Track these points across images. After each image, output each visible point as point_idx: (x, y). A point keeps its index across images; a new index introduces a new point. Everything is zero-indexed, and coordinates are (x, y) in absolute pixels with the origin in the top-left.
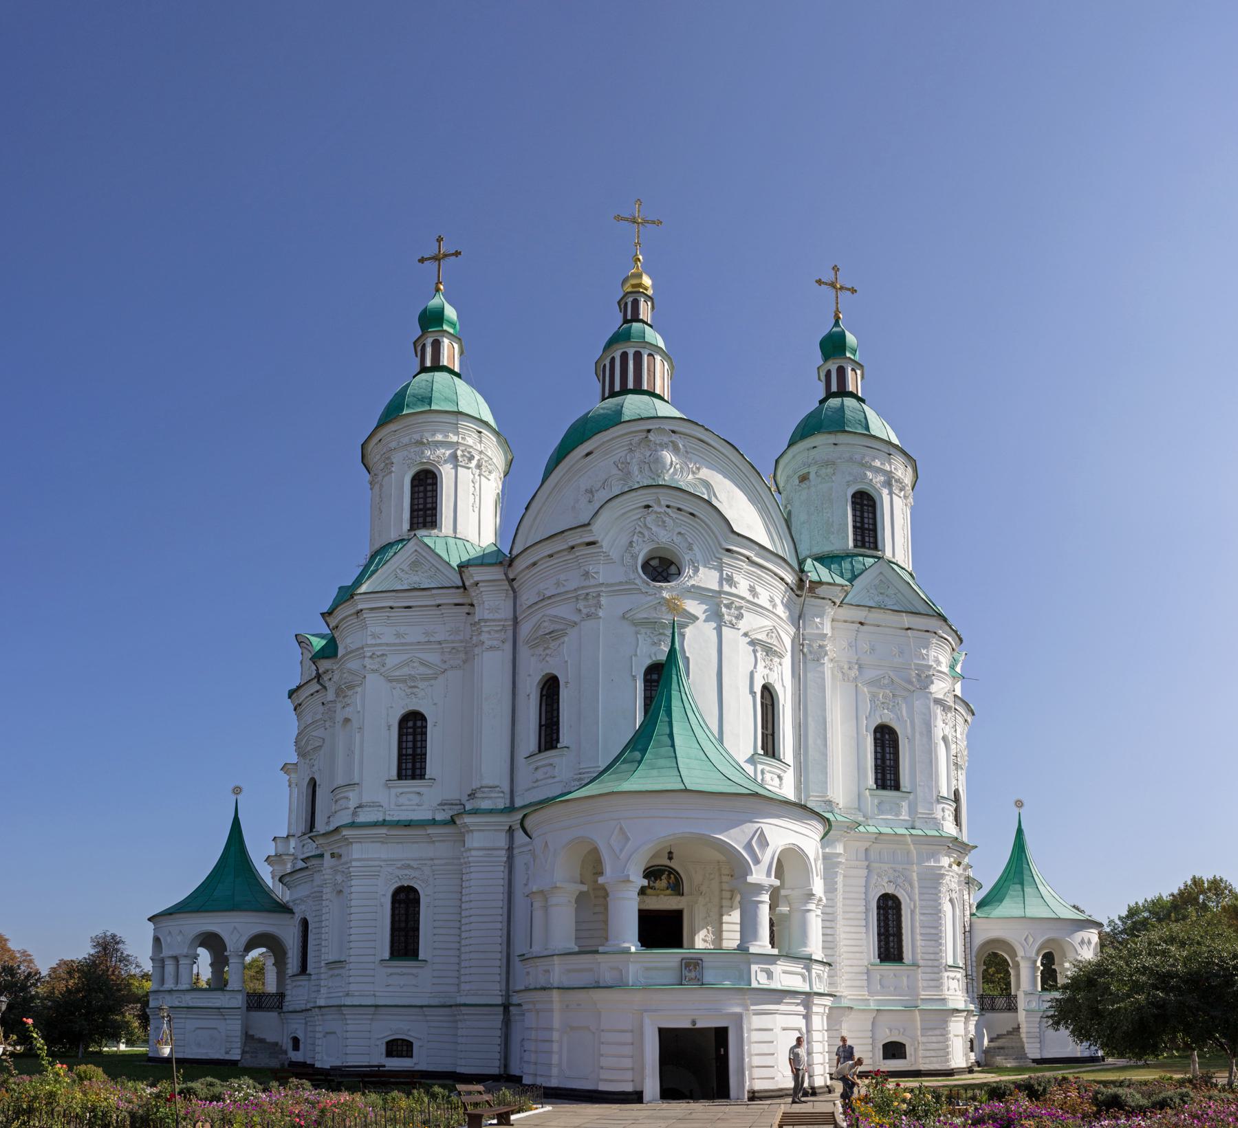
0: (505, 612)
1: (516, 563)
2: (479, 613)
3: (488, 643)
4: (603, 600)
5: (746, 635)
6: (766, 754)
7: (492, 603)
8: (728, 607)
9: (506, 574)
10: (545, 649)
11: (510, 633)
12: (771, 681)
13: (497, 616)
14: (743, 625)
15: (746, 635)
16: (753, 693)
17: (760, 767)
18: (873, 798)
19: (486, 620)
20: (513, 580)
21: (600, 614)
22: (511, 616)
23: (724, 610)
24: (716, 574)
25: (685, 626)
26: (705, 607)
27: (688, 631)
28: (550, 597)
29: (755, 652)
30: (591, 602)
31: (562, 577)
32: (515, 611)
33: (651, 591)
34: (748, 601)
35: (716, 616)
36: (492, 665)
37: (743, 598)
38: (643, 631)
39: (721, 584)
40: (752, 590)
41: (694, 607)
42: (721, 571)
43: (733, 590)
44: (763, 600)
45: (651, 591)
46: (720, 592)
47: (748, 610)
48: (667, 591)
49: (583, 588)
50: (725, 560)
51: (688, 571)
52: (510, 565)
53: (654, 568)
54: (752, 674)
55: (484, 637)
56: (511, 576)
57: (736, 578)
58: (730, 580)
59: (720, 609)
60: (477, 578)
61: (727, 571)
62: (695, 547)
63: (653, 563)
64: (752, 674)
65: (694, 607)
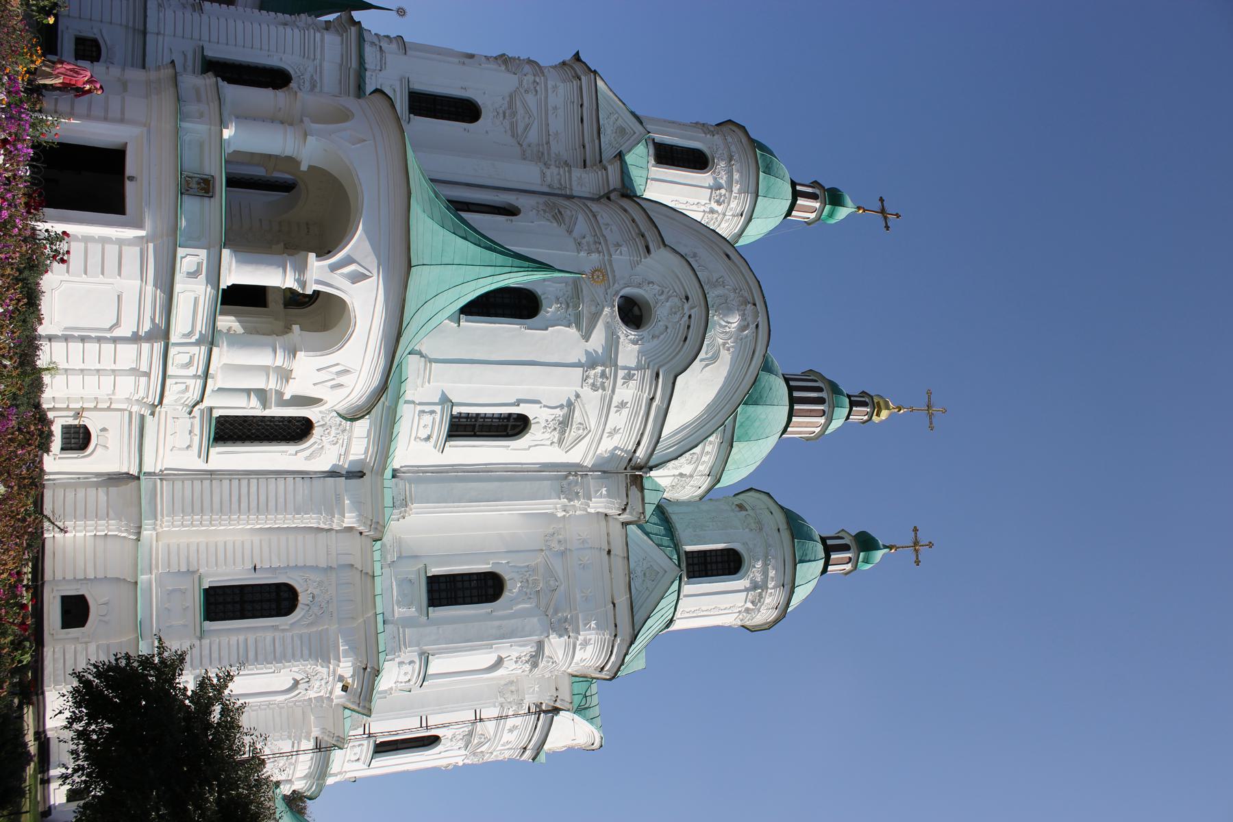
0: (577, 190)
1: (625, 200)
2: (577, 173)
3: (548, 173)
4: (595, 256)
5: (578, 396)
6: (452, 417)
7: (586, 182)
8: (603, 375)
9: (615, 190)
10: (545, 211)
11: (557, 192)
12: (533, 428)
13: (574, 184)
14: (586, 392)
15: (578, 396)
16: (518, 403)
17: (438, 409)
18: (412, 570)
19: (570, 172)
20: (609, 198)
21: (583, 254)
22: (575, 194)
23: (599, 369)
24: (633, 365)
25: (579, 328)
26: (600, 351)
27: (573, 331)
28: (595, 216)
29: (561, 406)
30: (593, 247)
31: (614, 228)
32: (580, 197)
33: (608, 298)
34: (611, 399)
35: (592, 362)
36: (529, 174)
37: (613, 391)
38: (569, 288)
39: (624, 368)
40: (623, 405)
41: (598, 339)
42: (639, 367)
43: (620, 381)
44: (618, 419)
45: (608, 298)
46: (616, 365)
47: (603, 398)
48: (610, 313)
49: (606, 240)
50: (648, 373)
51: (633, 334)
52: (624, 196)
53: (631, 310)
54: (538, 402)
55: (554, 170)
56: (613, 196)
57: (632, 383)
58: (629, 377)
59: (602, 363)
60: (609, 167)
61: (638, 375)
62: (656, 341)
63: (636, 309)
64: (538, 402)
65: (598, 339)
